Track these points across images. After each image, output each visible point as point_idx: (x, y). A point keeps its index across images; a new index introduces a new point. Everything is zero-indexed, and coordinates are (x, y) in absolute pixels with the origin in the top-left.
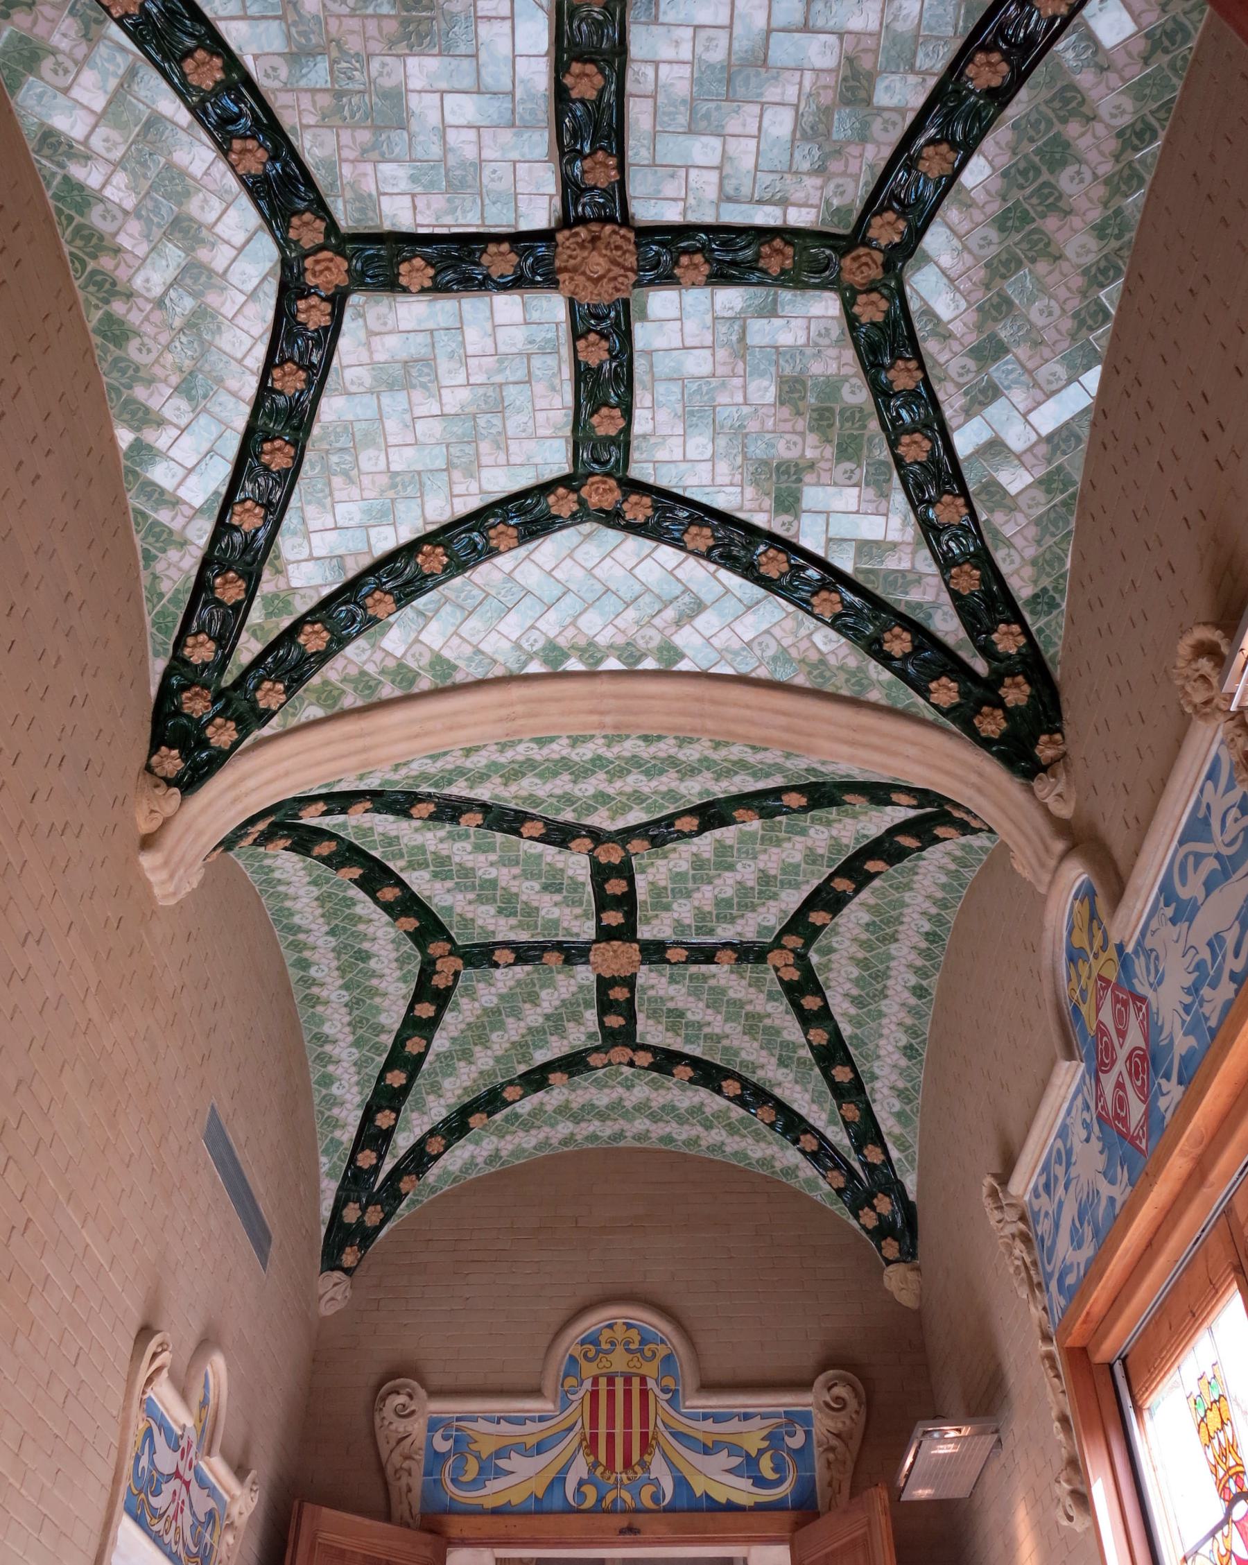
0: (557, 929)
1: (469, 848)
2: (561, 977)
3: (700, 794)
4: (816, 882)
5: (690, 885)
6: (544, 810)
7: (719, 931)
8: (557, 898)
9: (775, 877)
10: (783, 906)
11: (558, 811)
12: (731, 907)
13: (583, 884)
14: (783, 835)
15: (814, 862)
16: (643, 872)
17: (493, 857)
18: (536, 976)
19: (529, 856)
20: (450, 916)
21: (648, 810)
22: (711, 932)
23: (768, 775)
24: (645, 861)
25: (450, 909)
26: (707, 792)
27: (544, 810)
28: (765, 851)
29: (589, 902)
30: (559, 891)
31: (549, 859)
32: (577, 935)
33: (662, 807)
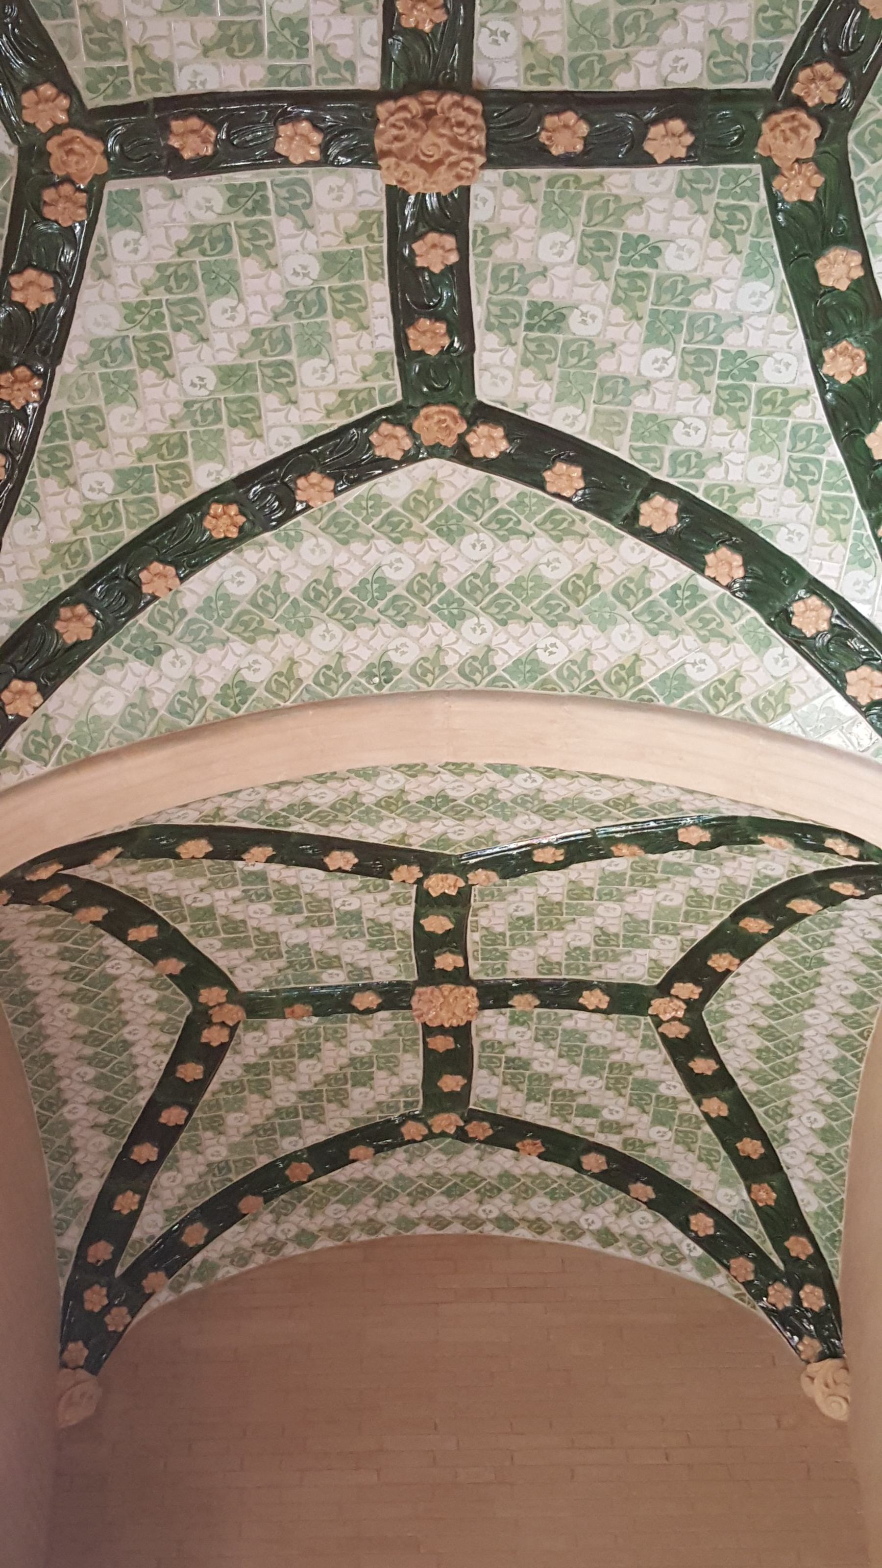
0: (549, 198)
1: (678, 430)
2: (555, 46)
3: (300, 538)
4: (66, 367)
5: (291, 322)
6: (543, 503)
7: (219, 202)
8: (539, 291)
9: (143, 365)
10: (107, 288)
11: (520, 502)
12: (207, 270)
13: (489, 327)
14: (153, 461)
15: (84, 414)
16: (379, 356)
17: (641, 402)
18: (612, 54)
19: (579, 399)
20: (755, 247)
21: (378, 501)
22: (235, 196)
23: (207, 607)
24: (377, 382)
25: (751, 272)
26: (290, 542)
27: (543, 503)
28: (174, 423)
29: (481, 280)
30: (536, 309)
31: (547, 391)
32: (508, 183)
33: (356, 506)
